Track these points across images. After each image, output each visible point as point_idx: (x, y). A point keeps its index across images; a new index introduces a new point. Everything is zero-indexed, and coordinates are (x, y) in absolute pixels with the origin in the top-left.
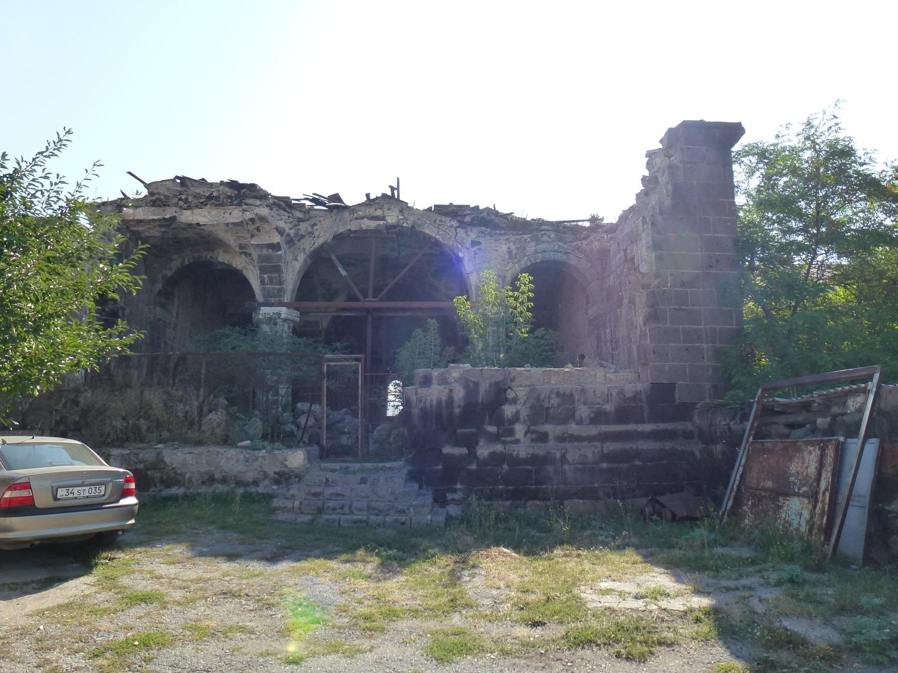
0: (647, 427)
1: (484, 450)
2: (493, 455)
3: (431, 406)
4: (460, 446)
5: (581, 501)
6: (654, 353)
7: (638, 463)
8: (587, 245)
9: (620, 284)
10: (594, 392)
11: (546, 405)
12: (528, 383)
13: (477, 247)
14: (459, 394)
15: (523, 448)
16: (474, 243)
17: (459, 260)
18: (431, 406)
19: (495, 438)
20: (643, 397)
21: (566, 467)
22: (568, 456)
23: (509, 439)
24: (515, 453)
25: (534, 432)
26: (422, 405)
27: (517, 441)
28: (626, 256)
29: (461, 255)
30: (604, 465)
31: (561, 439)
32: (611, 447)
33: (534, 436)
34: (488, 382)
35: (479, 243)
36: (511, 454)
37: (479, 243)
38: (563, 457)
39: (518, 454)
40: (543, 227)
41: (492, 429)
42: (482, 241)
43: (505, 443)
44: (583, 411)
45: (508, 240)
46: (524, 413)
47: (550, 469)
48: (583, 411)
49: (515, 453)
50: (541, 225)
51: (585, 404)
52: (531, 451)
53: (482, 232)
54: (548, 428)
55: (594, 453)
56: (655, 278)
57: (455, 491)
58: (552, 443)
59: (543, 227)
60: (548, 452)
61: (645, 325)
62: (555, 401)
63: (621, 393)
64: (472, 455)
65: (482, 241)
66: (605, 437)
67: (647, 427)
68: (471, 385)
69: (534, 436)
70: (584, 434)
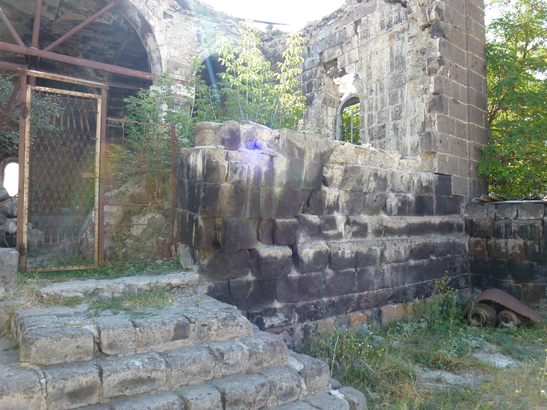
0: (436, 220)
1: (308, 250)
2: (319, 255)
3: (248, 179)
4: (278, 244)
5: (395, 306)
6: (441, 142)
7: (433, 258)
8: (270, 47)
9: (310, 86)
10: (402, 177)
11: (365, 190)
12: (342, 160)
13: (169, 20)
14: (281, 165)
15: (347, 248)
16: (166, 15)
17: (148, 29)
18: (248, 179)
19: (317, 232)
20: (433, 187)
21: (385, 267)
22: (387, 254)
23: (331, 232)
24: (340, 252)
25: (355, 223)
26: (236, 177)
27: (339, 236)
28: (321, 60)
29: (151, 23)
30: (412, 262)
31: (378, 232)
32: (418, 240)
33: (355, 229)
34: (313, 151)
35: (171, 17)
36: (337, 253)
37: (171, 17)
38: (382, 254)
39: (343, 253)
40: (229, 20)
41: (314, 219)
42: (174, 15)
43: (327, 238)
44: (393, 201)
45: (198, 22)
46: (344, 198)
47: (371, 269)
48: (393, 201)
49: (340, 252)
50: (226, 18)
51: (393, 190)
52: (355, 248)
53: (173, 7)
54: (365, 218)
55: (405, 248)
56: (440, 65)
57: (273, 312)
58: (370, 237)
59: (229, 20)
60: (370, 250)
61: (429, 111)
62: (373, 185)
63: (420, 181)
64: (296, 258)
65: (174, 15)
66: (412, 230)
67: (436, 220)
68: (296, 152)
69: (355, 229)
70: (396, 226)
